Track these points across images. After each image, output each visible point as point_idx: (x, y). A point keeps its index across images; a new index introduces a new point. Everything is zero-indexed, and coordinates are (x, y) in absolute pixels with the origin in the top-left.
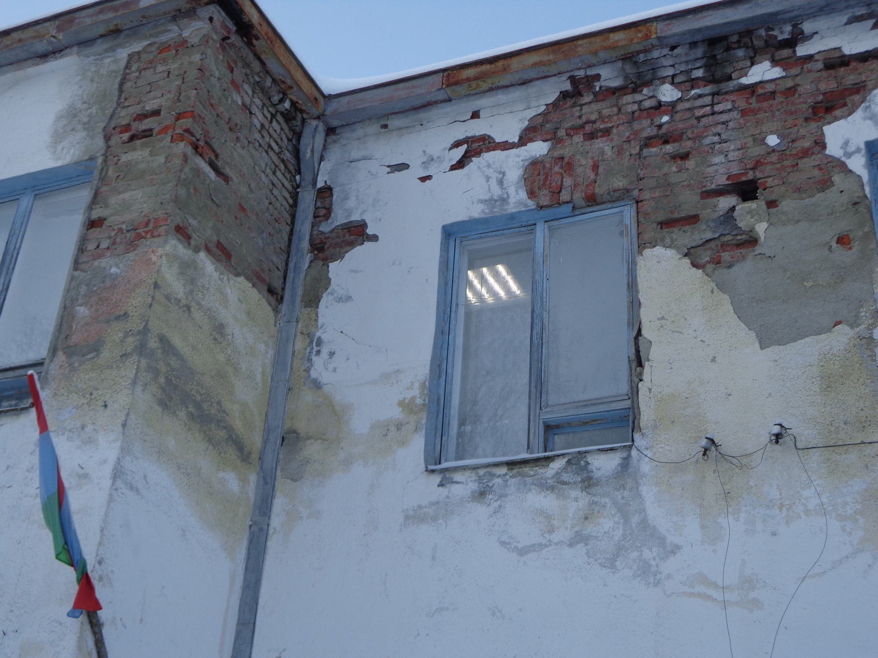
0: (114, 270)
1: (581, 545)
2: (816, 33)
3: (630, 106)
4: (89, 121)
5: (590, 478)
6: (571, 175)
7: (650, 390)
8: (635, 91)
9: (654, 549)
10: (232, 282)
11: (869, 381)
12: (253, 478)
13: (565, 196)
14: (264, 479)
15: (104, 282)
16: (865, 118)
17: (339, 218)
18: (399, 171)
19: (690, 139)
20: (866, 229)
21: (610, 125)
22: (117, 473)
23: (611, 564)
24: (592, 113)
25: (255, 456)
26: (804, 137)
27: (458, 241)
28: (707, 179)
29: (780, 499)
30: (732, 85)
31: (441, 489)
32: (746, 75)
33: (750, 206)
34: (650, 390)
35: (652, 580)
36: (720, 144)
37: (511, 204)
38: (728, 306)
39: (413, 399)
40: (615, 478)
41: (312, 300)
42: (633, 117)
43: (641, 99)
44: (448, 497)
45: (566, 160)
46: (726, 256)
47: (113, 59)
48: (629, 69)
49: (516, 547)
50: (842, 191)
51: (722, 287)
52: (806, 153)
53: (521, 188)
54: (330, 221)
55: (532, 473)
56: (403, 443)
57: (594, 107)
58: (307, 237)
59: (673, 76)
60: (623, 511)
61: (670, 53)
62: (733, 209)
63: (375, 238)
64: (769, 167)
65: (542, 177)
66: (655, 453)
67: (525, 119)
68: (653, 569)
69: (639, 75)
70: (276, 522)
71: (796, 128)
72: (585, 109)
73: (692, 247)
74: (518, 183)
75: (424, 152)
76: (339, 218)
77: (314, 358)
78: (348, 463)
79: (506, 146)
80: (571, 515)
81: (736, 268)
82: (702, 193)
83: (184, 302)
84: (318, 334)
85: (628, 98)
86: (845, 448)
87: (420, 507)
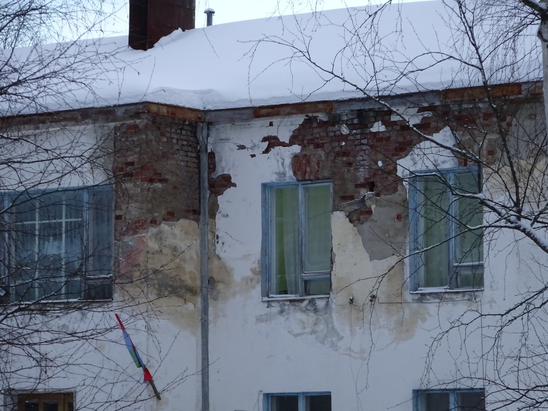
0: (130, 243)
1: (314, 334)
6: (309, 166)
7: (335, 275)
10: (176, 226)
12: (199, 300)
13: (307, 177)
14: (204, 299)
15: (128, 248)
16: (411, 159)
17: (219, 172)
18: (242, 149)
19: (352, 156)
21: (323, 142)
24: (317, 133)
25: (199, 290)
27: (269, 189)
30: (367, 131)
32: (372, 127)
34: (335, 275)
39: (255, 268)
41: (213, 216)
44: (270, 312)
45: (307, 157)
46: (362, 217)
49: (293, 334)
51: (360, 232)
54: (215, 172)
56: (253, 288)
57: (318, 130)
58: (207, 180)
59: (347, 120)
63: (234, 185)
64: (378, 177)
65: (298, 164)
68: (335, 345)
70: (211, 318)
72: (315, 131)
74: (289, 166)
75: (252, 141)
76: (219, 172)
77: (217, 245)
78: (234, 294)
79: (284, 144)
83: (159, 250)
84: (217, 233)
85: (330, 128)
87: (261, 315)
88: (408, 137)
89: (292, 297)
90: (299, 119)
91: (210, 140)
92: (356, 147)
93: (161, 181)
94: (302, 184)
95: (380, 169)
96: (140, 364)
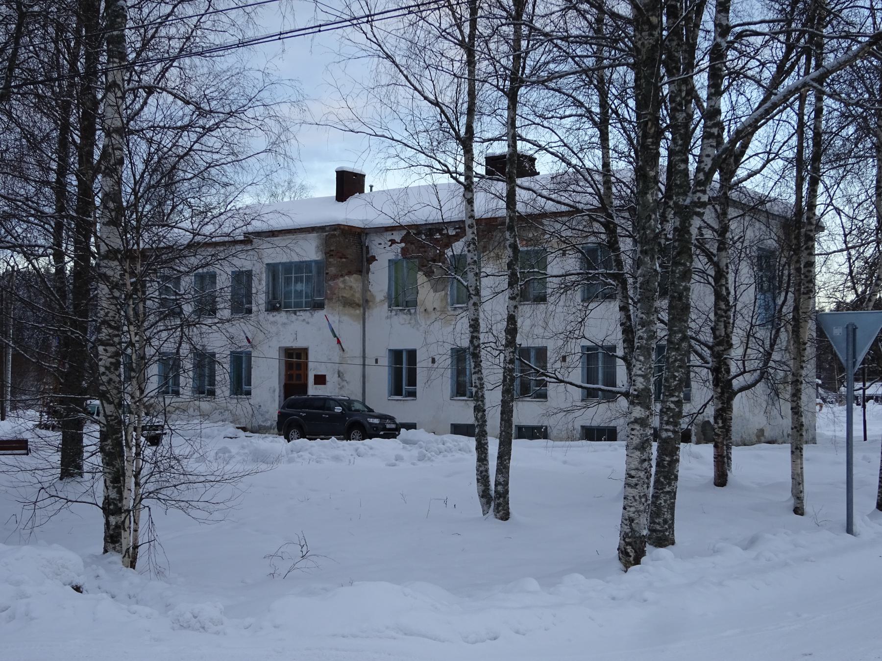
12: (362, 309)
22: (339, 321)
41: (368, 273)
79: (398, 243)
89: (401, 308)
90: (404, 232)
91: (367, 241)
93: (345, 258)
96: (335, 336)
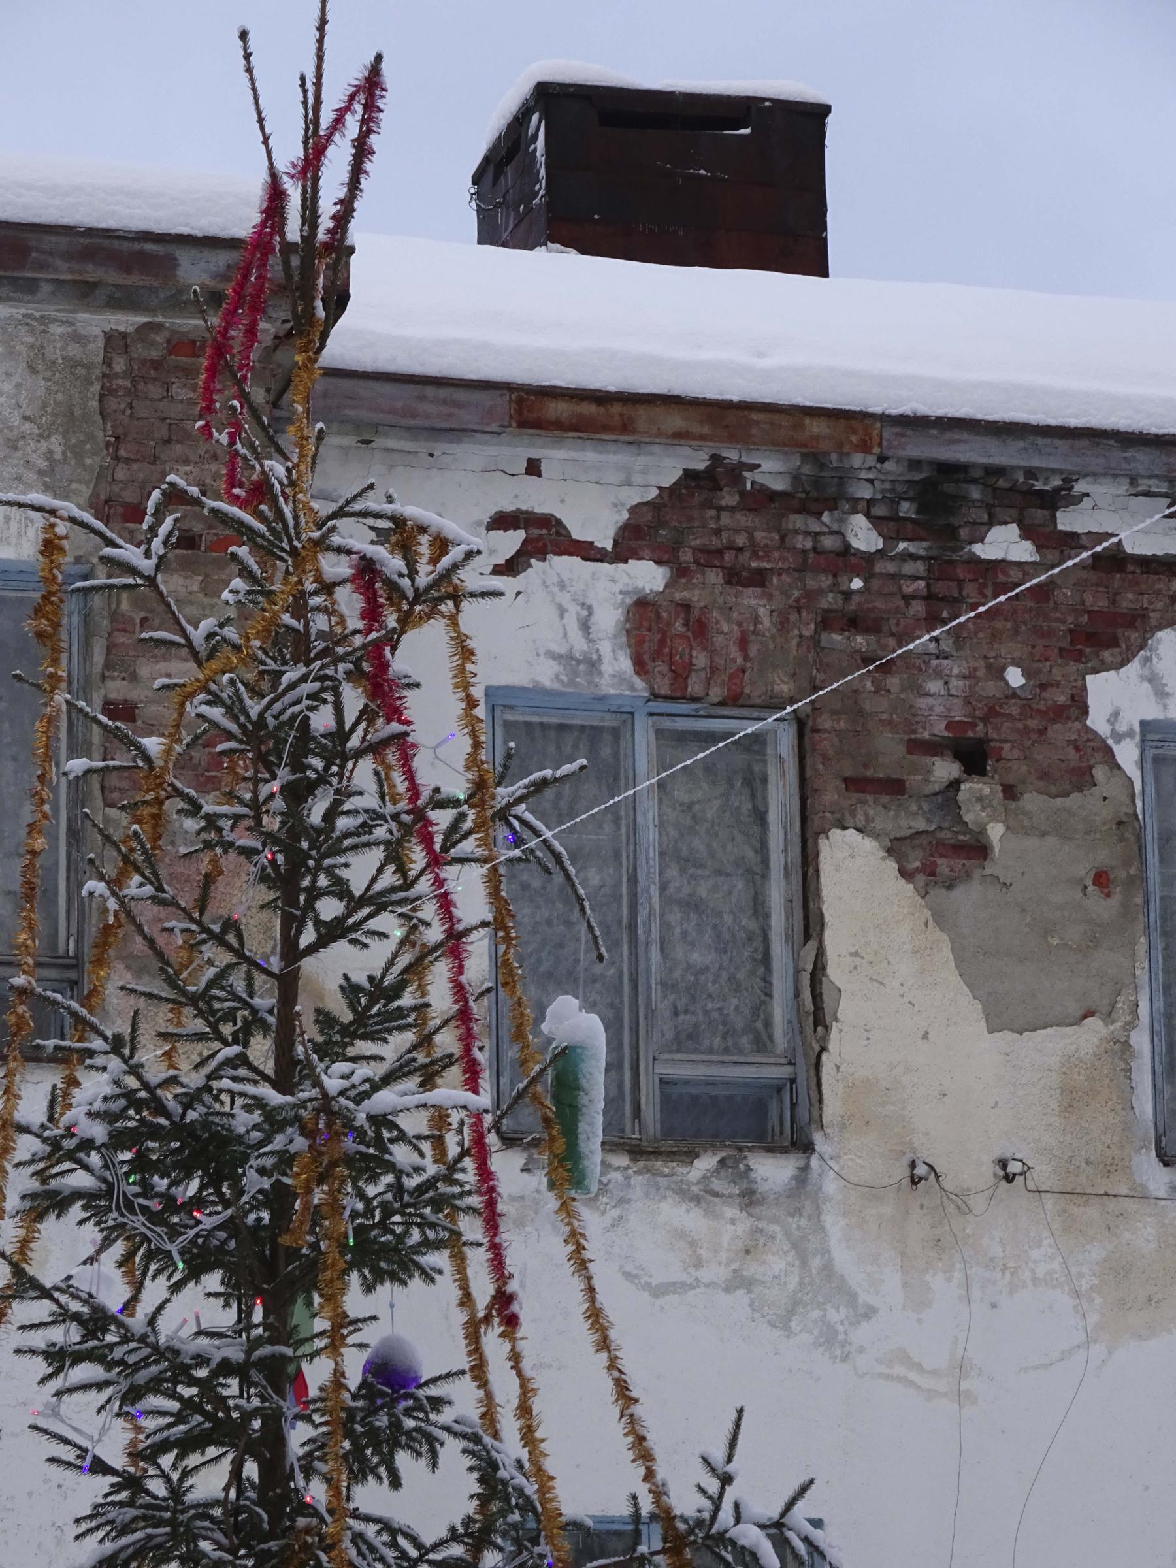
1: (742, 1291)
2: (1088, 495)
3: (800, 538)
4: (51, 470)
5: (752, 1192)
6: (705, 649)
7: (838, 1067)
8: (802, 509)
9: (842, 1310)
11: (1120, 1107)
13: (695, 686)
16: (1142, 678)
19: (892, 635)
20: (1133, 871)
21: (765, 565)
23: (783, 1323)
24: (737, 531)
26: (1058, 684)
28: (917, 719)
29: (1003, 1258)
31: (525, 1175)
32: (982, 540)
33: (981, 790)
34: (838, 1067)
35: (838, 1352)
36: (938, 658)
37: (606, 676)
38: (947, 953)
40: (788, 1197)
42: (805, 560)
43: (818, 530)
45: (697, 613)
46: (943, 866)
47: (69, 330)
48: (807, 469)
49: (648, 1284)
50: (1105, 799)
51: (941, 919)
52: (1058, 714)
53: (621, 648)
55: (666, 1171)
57: (744, 520)
59: (870, 502)
60: (798, 1246)
61: (879, 466)
62: (955, 785)
64: (1008, 724)
66: (843, 1168)
67: (623, 505)
68: (841, 1337)
69: (817, 482)
71: (1048, 664)
72: (726, 519)
73: (896, 839)
74: (615, 637)
79: (587, 552)
80: (725, 1244)
81: (959, 892)
82: (910, 740)
85: (797, 521)
86: (1085, 1198)
88: (1128, 600)
92: (908, 605)
94: (651, 714)
95: (1013, 694)
